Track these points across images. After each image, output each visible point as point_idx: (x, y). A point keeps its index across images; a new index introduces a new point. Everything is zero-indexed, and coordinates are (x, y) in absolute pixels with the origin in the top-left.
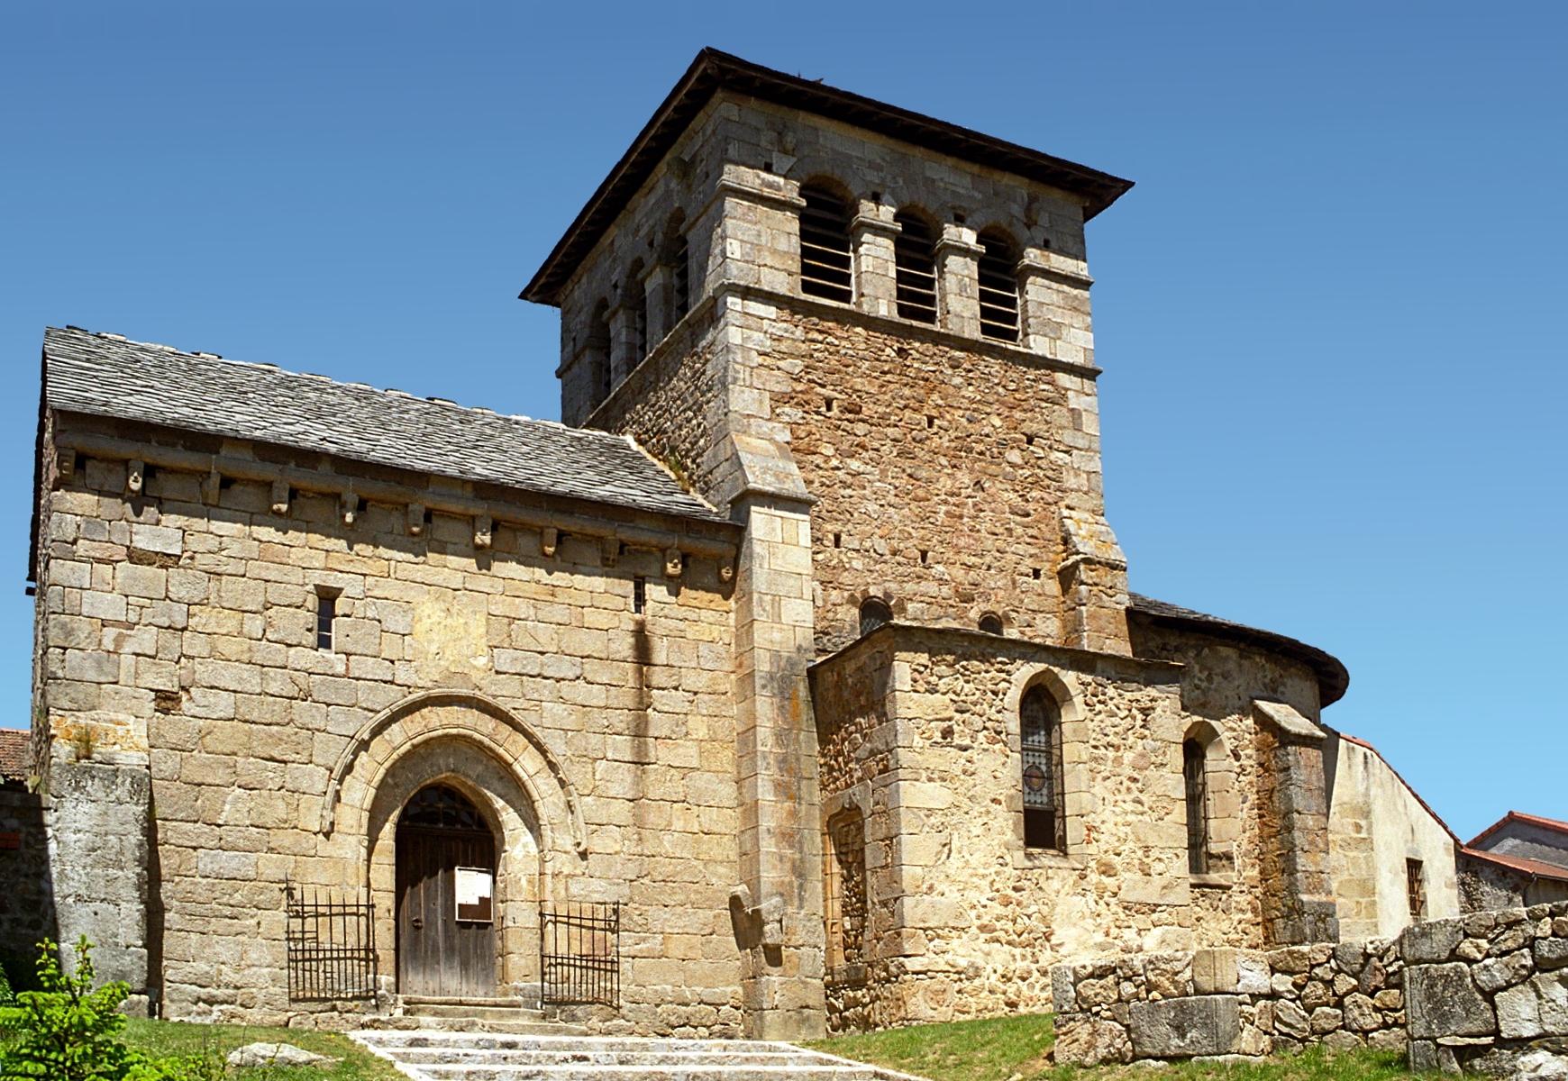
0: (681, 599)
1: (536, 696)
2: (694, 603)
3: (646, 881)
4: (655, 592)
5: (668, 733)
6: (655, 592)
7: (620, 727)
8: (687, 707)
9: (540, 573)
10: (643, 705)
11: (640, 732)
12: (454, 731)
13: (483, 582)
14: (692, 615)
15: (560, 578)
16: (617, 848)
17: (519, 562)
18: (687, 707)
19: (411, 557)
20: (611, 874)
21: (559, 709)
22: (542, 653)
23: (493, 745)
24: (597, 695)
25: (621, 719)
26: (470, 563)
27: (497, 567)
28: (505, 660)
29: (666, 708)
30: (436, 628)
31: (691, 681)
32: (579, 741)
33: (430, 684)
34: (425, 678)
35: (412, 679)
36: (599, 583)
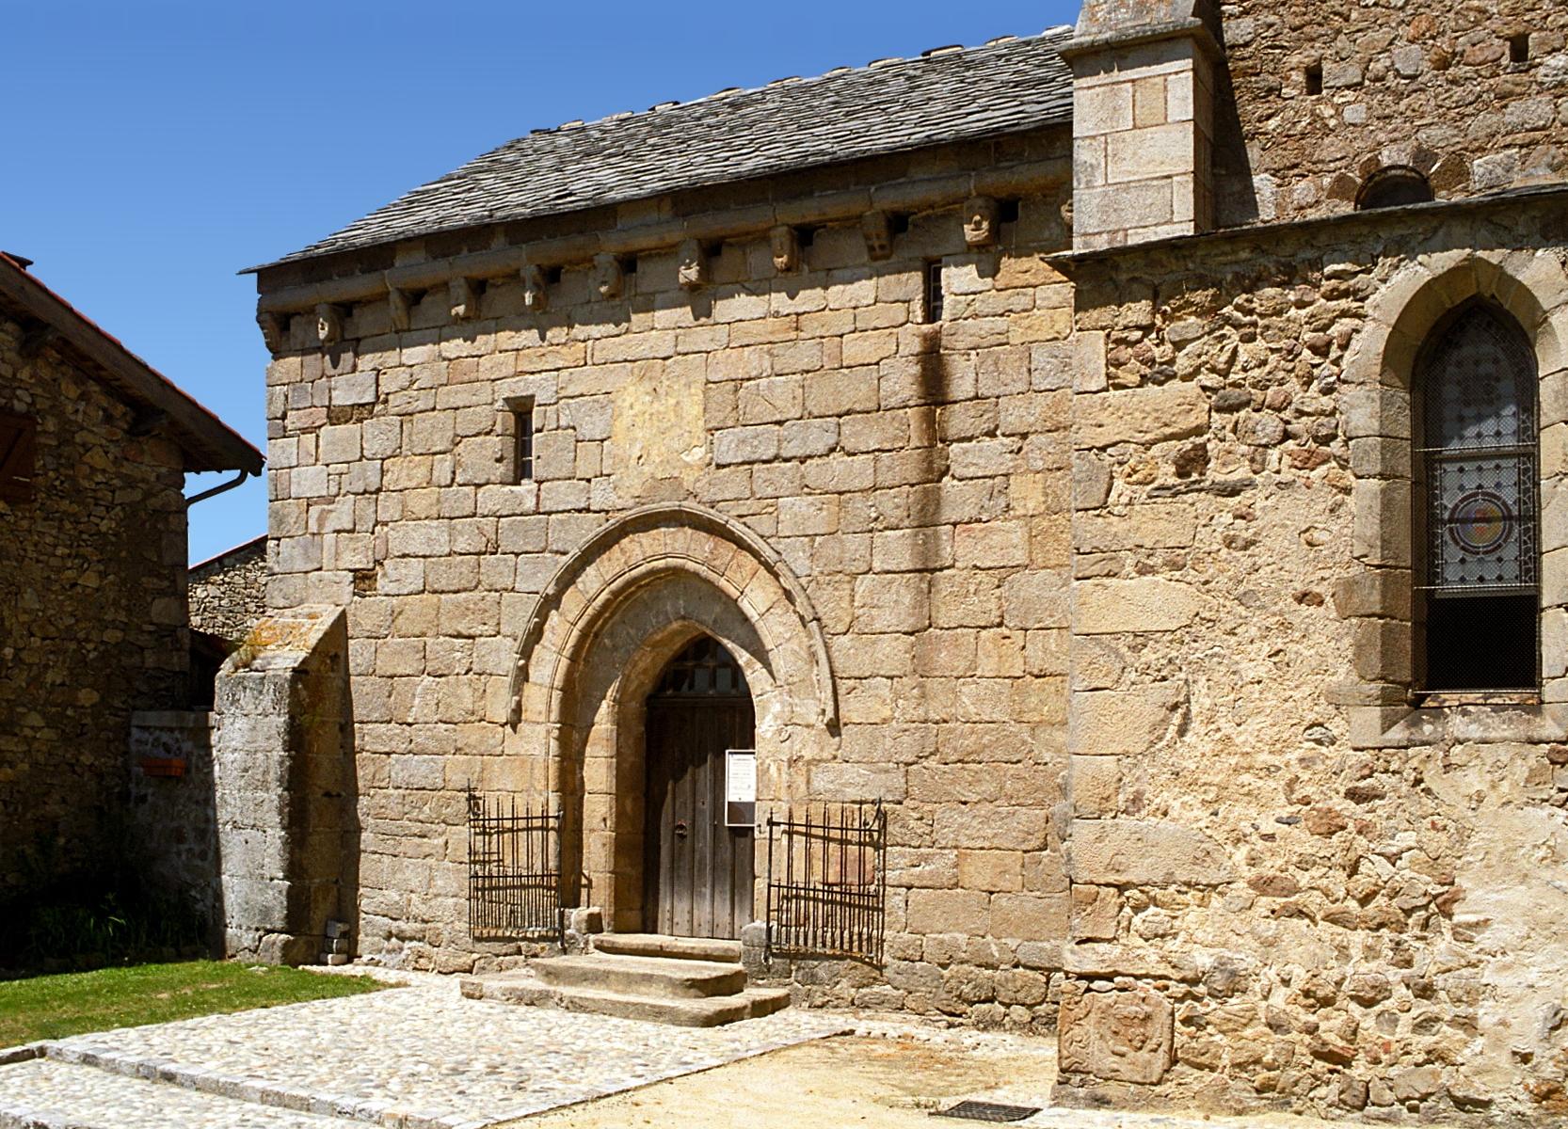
0: (1002, 279)
1: (770, 491)
2: (1029, 278)
3: (932, 763)
4: (958, 279)
5: (974, 513)
6: (958, 279)
7: (894, 515)
8: (1009, 462)
9: (779, 300)
10: (935, 472)
11: (927, 517)
12: (661, 564)
13: (702, 337)
14: (1021, 301)
15: (809, 298)
16: (886, 713)
17: (751, 293)
18: (1009, 462)
19: (611, 328)
20: (876, 755)
21: (802, 504)
22: (780, 423)
23: (713, 576)
24: (851, 471)
25: (893, 504)
26: (684, 315)
27: (723, 309)
28: (728, 446)
29: (971, 472)
30: (639, 421)
31: (1015, 415)
32: (831, 550)
33: (631, 503)
34: (620, 496)
35: (613, 500)
36: (864, 290)
